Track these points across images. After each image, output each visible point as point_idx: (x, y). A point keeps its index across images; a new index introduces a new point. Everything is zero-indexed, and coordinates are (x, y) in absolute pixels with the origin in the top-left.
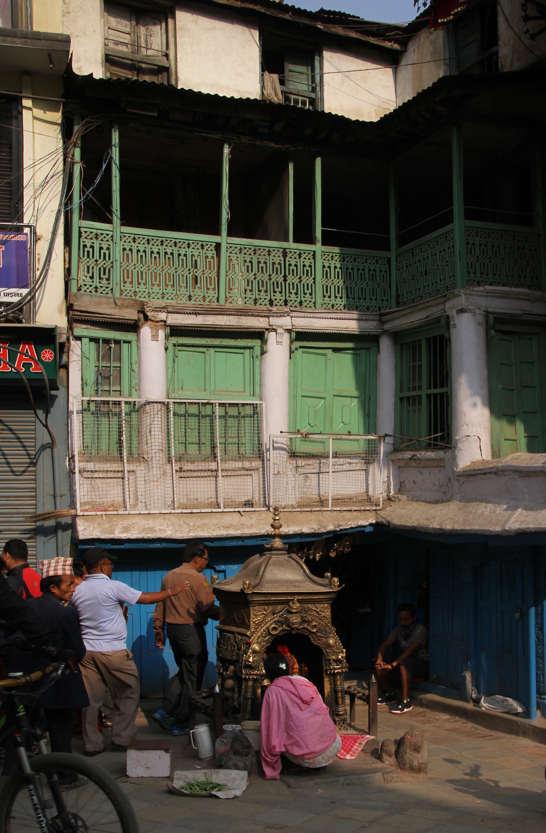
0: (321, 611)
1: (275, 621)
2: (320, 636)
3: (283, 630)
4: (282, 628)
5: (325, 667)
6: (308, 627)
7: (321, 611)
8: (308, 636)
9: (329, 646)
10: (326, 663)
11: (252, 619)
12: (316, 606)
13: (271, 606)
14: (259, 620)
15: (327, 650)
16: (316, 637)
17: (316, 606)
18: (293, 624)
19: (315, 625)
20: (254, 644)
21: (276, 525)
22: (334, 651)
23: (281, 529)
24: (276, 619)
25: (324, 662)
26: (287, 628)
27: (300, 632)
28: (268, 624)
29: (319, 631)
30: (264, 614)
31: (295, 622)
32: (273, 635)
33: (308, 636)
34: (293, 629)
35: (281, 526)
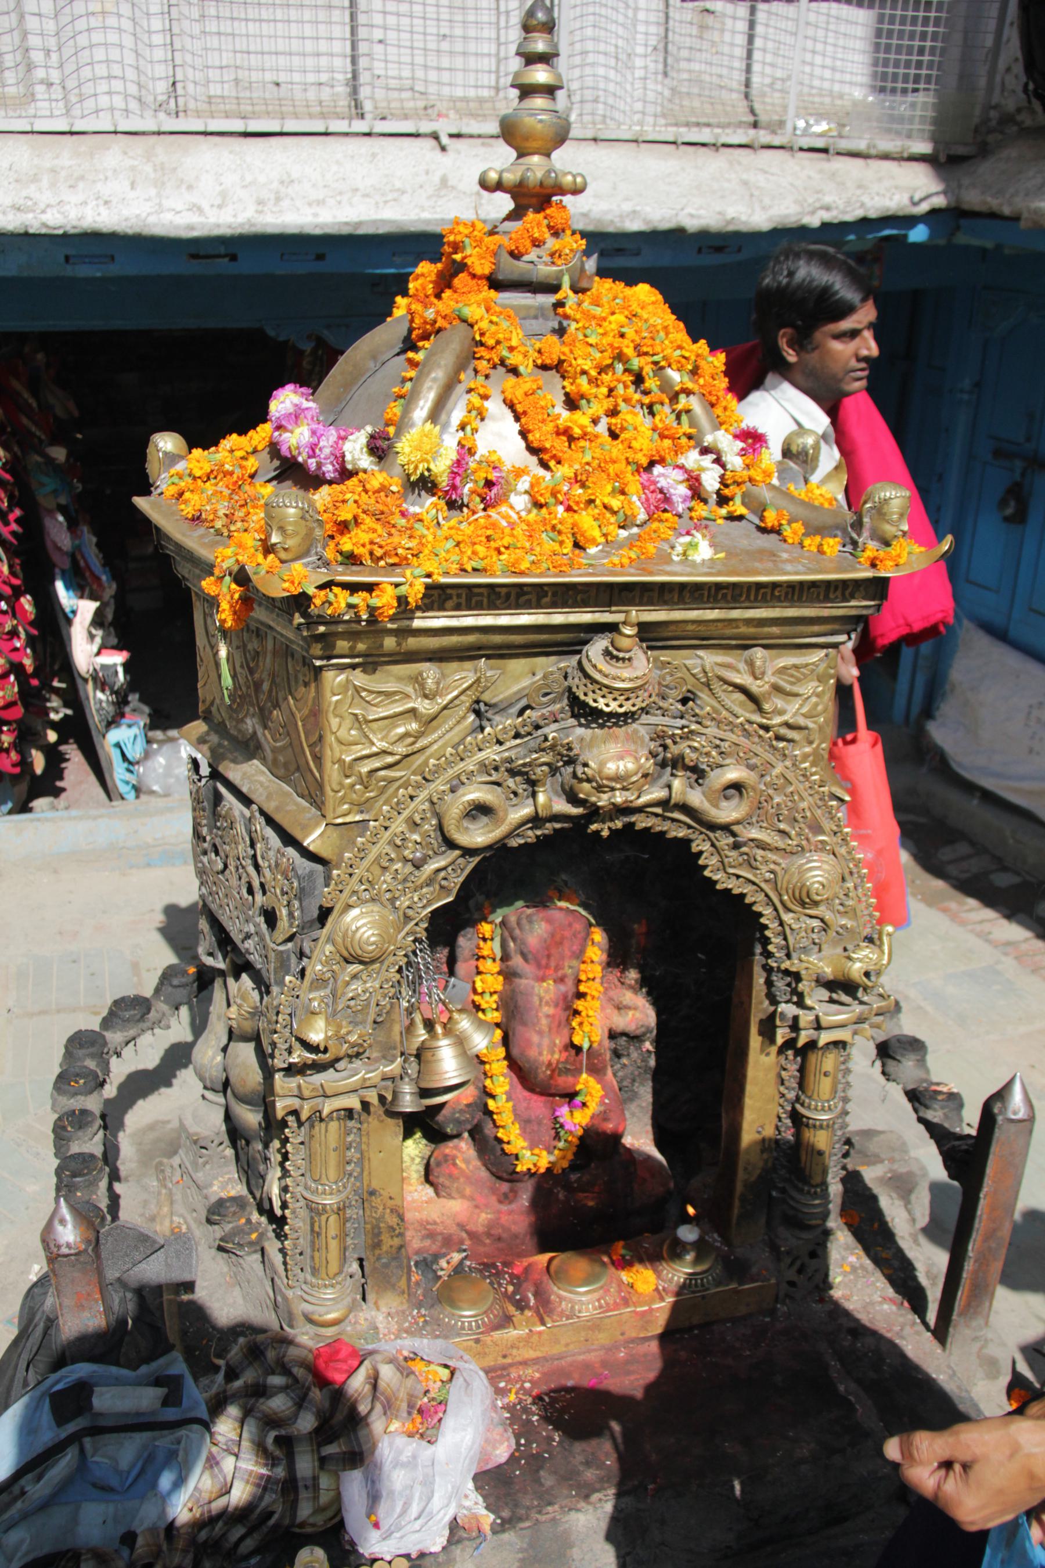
0: (777, 689)
1: (484, 767)
2: (762, 846)
3: (536, 820)
4: (526, 811)
5: (761, 1006)
6: (696, 798)
7: (777, 689)
8: (687, 842)
9: (805, 900)
10: (769, 983)
11: (332, 751)
12: (751, 664)
13: (468, 665)
14: (385, 752)
15: (787, 917)
16: (736, 846)
17: (751, 664)
18: (600, 789)
19: (737, 787)
20: (349, 907)
21: (529, 121)
22: (826, 926)
23: (558, 156)
24: (492, 754)
25: (759, 979)
26: (562, 806)
27: (642, 822)
28: (439, 785)
29: (759, 811)
30: (413, 711)
31: (617, 778)
32: (468, 852)
33: (687, 842)
34: (594, 813)
35: (560, 137)
